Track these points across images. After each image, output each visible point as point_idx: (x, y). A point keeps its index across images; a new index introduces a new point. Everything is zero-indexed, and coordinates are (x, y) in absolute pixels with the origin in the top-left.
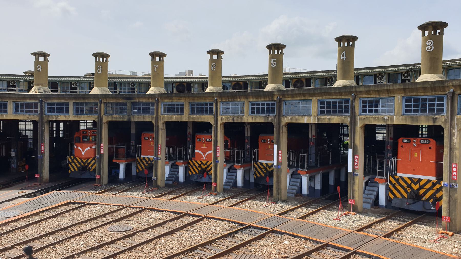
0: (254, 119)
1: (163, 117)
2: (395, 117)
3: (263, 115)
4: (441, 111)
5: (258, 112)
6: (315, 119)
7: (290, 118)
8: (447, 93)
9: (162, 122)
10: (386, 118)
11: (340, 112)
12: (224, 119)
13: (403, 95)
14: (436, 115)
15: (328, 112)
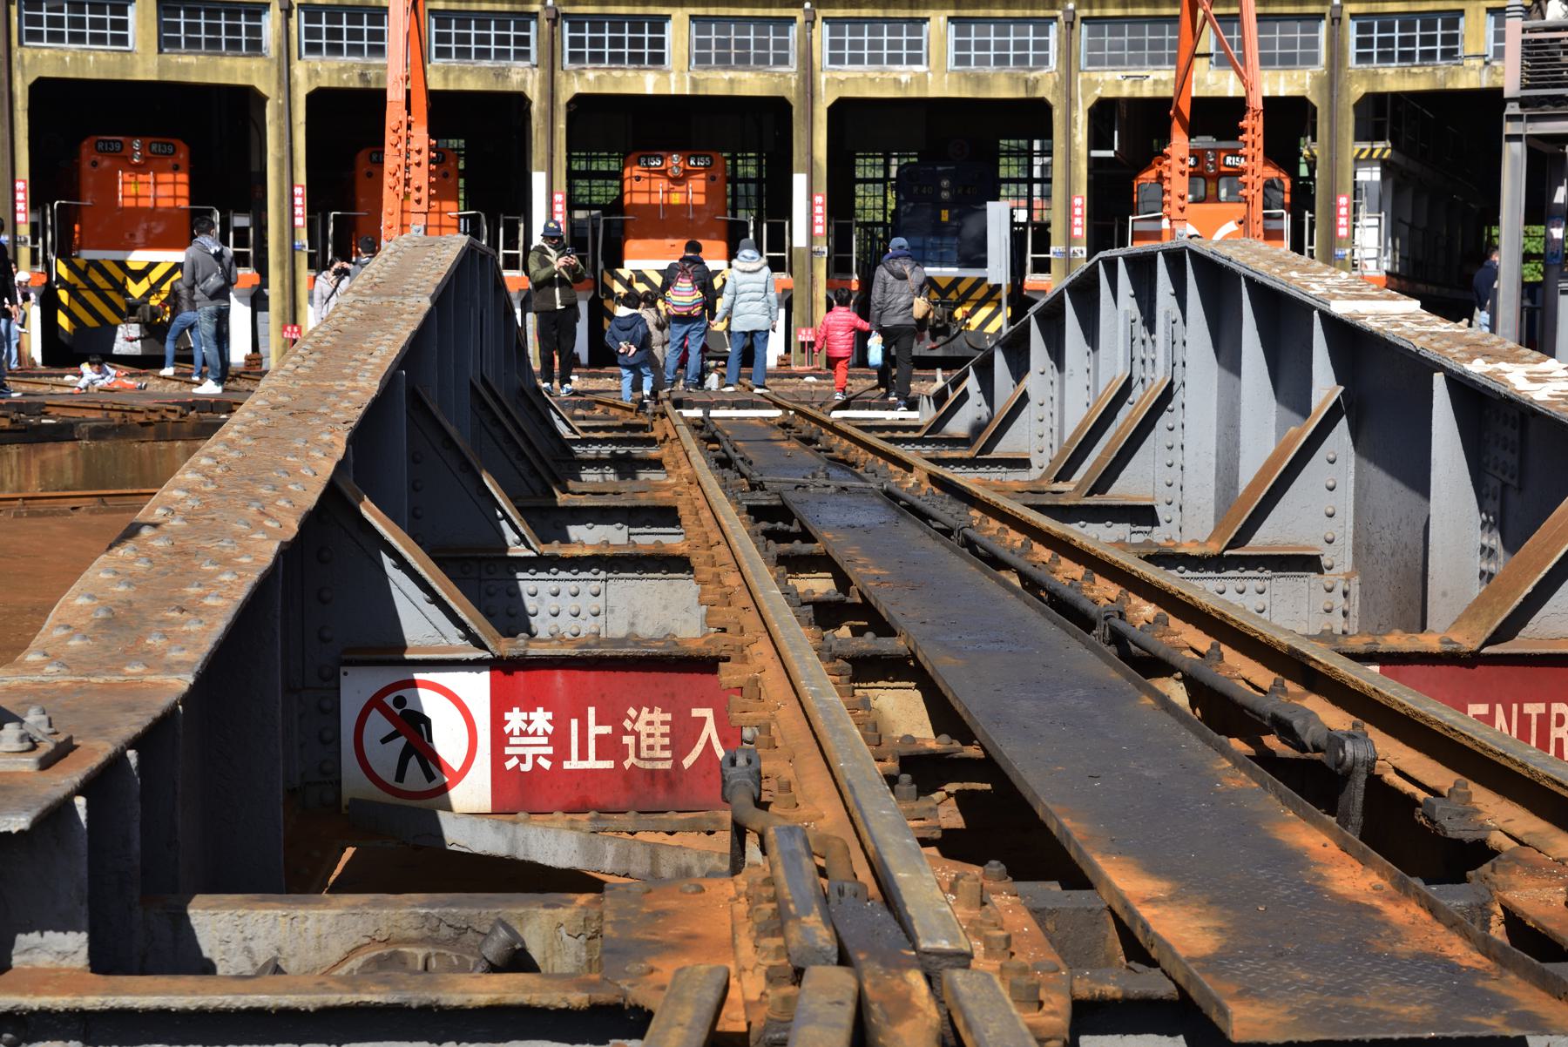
0: (451, 77)
1: (35, 57)
2: (930, 75)
3: (486, 63)
4: (1042, 61)
5: (463, 53)
6: (682, 80)
7: (591, 75)
8: (1059, 13)
9: (30, 80)
10: (904, 78)
11: (762, 60)
12: (325, 74)
13: (952, 13)
14: (1031, 70)
15: (723, 61)
